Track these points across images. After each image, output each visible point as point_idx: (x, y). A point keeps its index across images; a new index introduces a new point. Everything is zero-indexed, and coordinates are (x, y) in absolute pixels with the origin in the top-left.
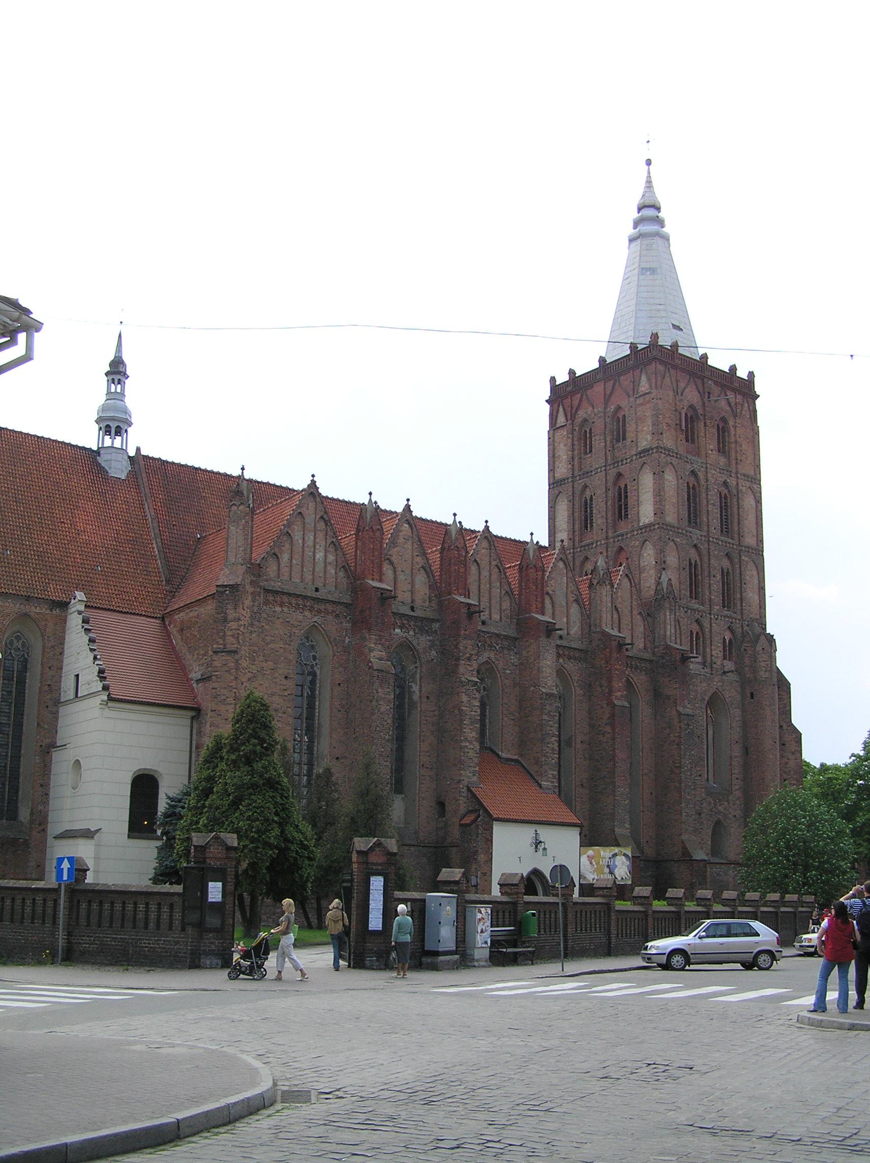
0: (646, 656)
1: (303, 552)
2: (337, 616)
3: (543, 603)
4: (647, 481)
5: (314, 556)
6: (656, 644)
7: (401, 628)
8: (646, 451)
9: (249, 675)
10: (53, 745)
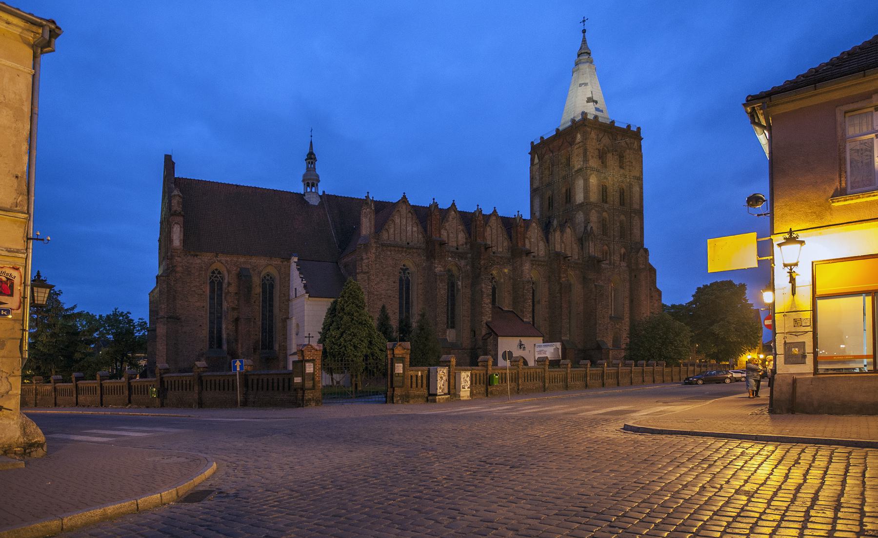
0: (580, 261)
1: (400, 228)
2: (419, 255)
3: (524, 241)
4: (580, 183)
5: (406, 229)
6: (585, 256)
7: (452, 257)
8: (580, 170)
9: (376, 282)
10: (288, 318)
